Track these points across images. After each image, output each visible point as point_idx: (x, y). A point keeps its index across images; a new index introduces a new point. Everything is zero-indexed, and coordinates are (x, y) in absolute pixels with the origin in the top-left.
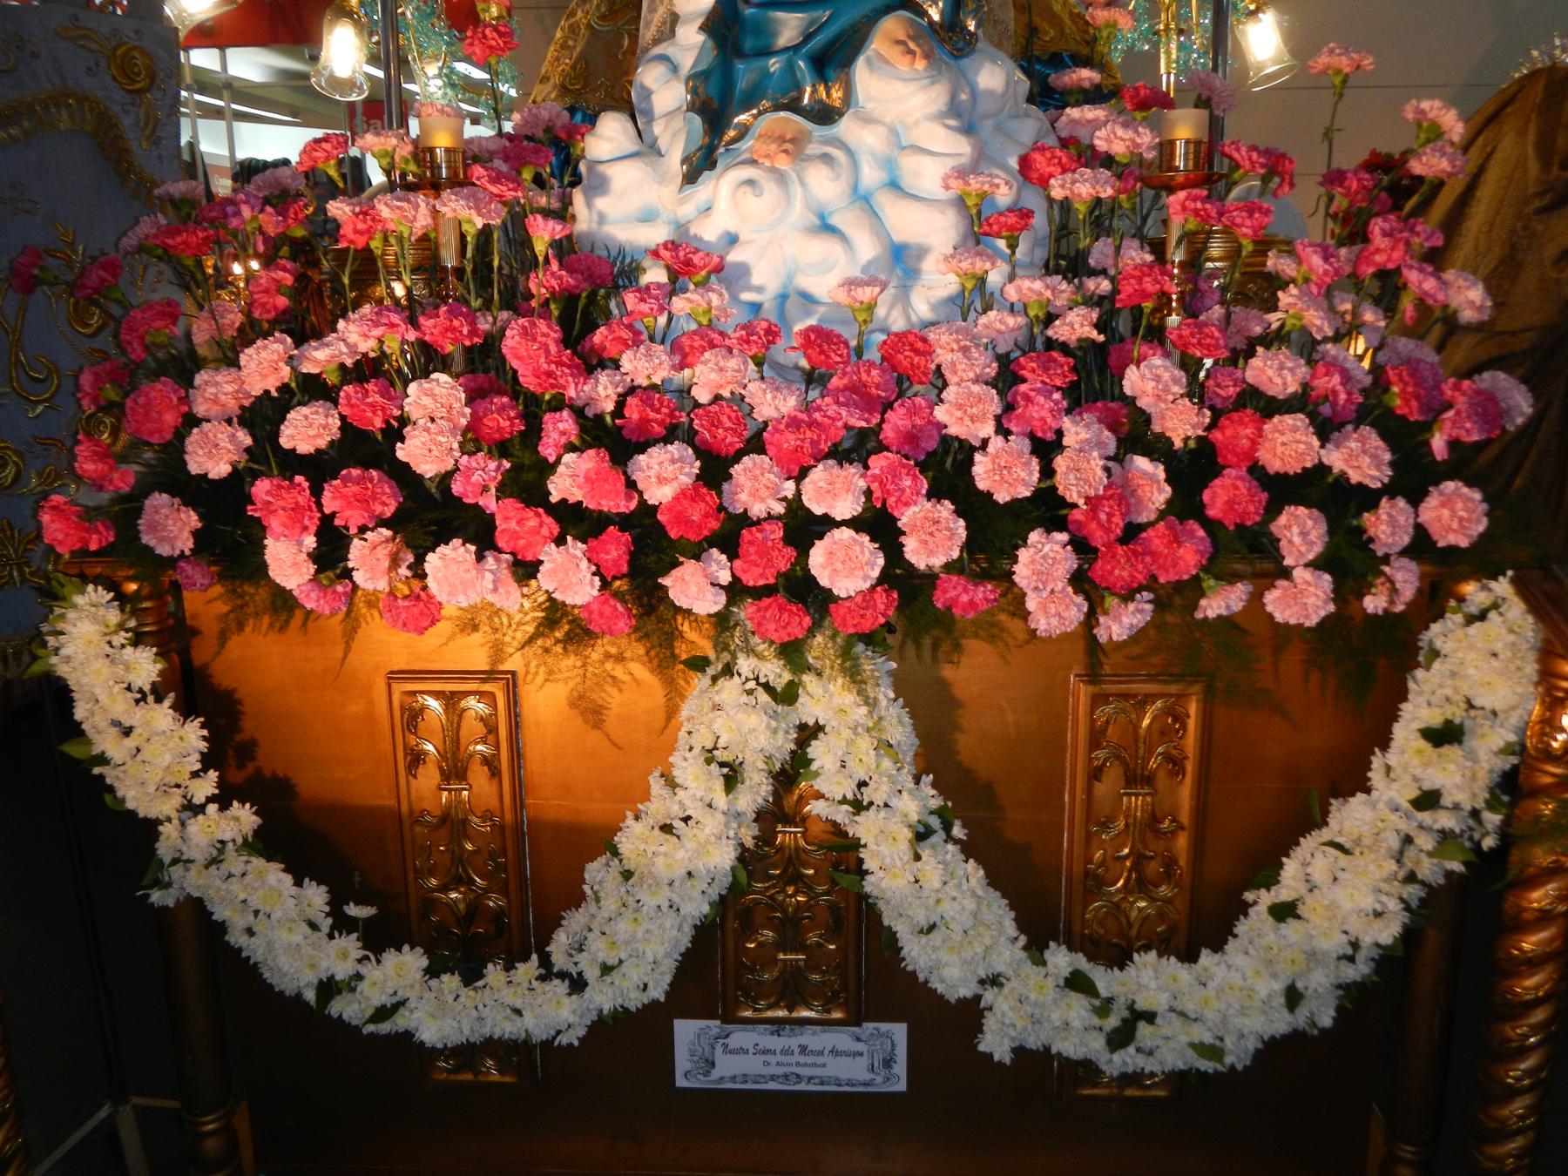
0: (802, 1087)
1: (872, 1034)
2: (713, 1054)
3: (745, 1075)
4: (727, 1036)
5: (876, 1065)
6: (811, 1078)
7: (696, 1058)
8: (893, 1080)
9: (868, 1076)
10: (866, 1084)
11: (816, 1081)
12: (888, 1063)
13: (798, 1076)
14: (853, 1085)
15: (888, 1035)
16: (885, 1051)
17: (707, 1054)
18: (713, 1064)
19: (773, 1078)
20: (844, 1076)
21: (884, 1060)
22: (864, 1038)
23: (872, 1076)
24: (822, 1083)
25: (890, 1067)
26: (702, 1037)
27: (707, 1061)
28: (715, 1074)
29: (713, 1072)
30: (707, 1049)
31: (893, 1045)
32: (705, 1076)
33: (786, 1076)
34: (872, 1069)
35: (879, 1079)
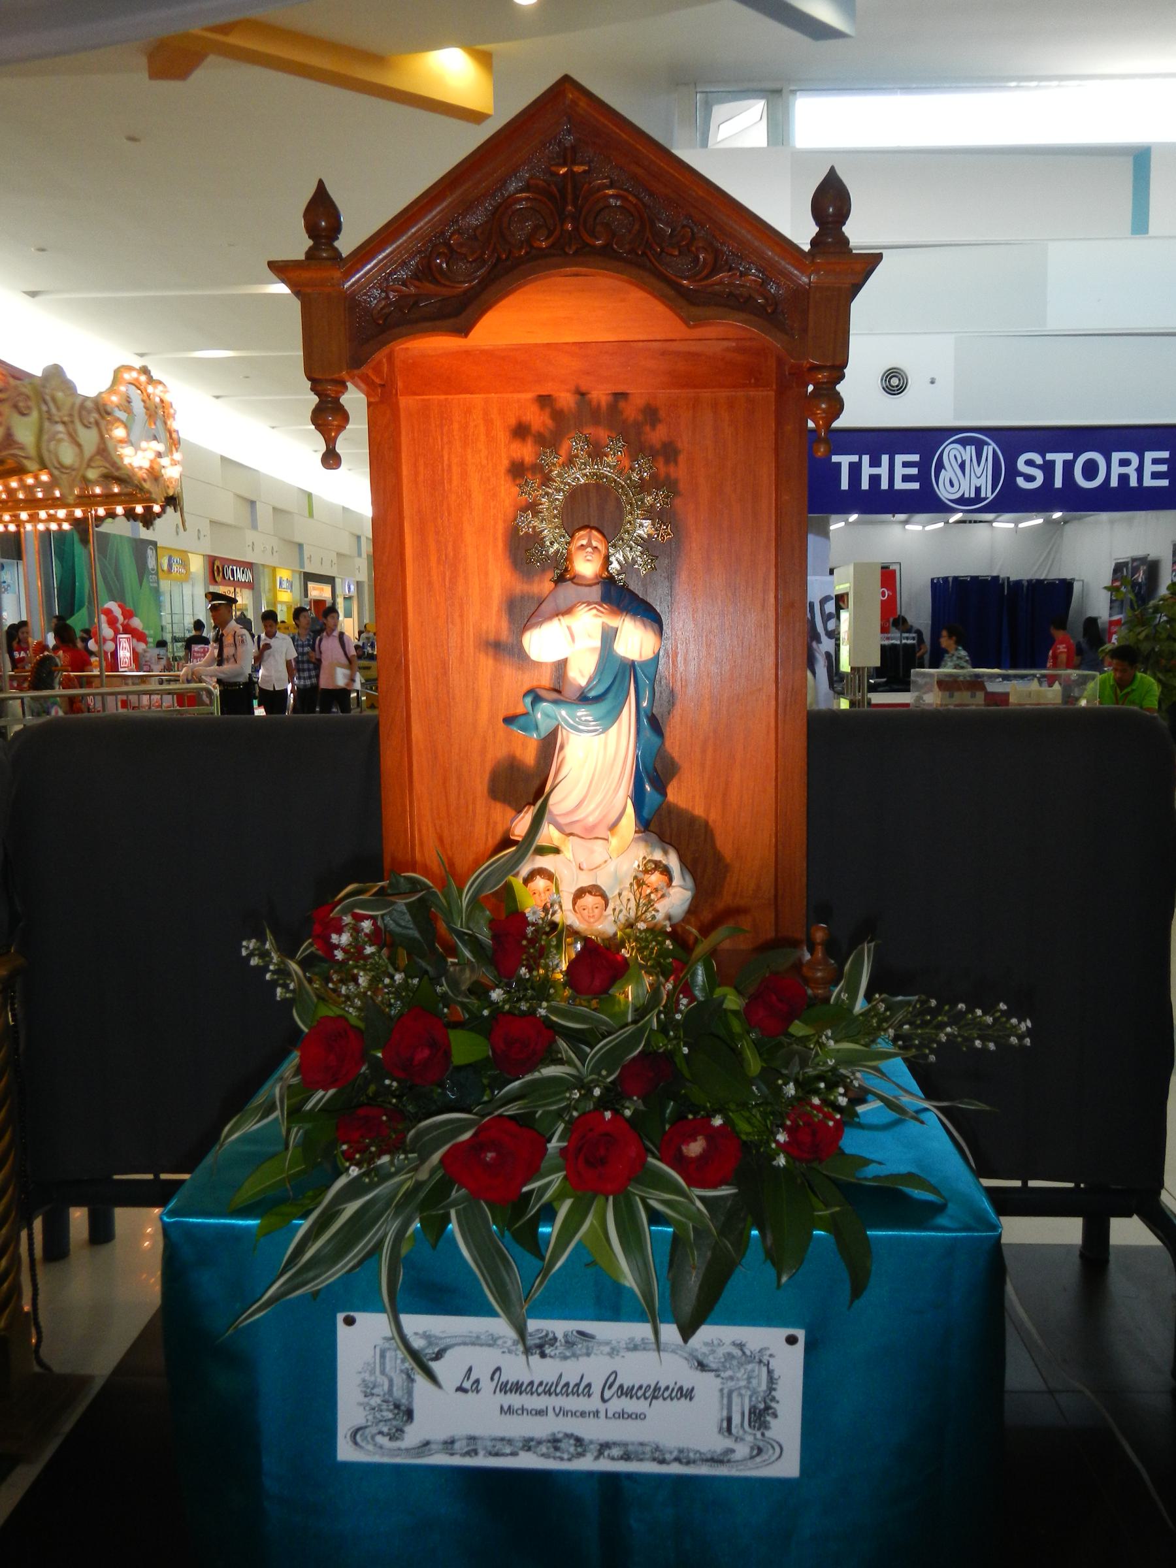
0: (586, 1464)
1: (730, 1356)
2: (410, 1393)
3: (472, 1439)
5: (736, 1420)
6: (604, 1447)
7: (375, 1401)
8: (770, 1454)
9: (718, 1443)
10: (714, 1460)
11: (616, 1452)
12: (760, 1416)
13: (579, 1441)
14: (688, 1463)
15: (761, 1359)
16: (754, 1392)
17: (398, 1393)
18: (409, 1414)
19: (528, 1444)
20: (670, 1441)
21: (753, 1410)
22: (714, 1366)
23: (728, 1443)
24: (626, 1457)
25: (764, 1426)
26: (388, 1354)
27: (397, 1406)
28: (413, 1435)
29: (408, 1429)
30: (399, 1380)
32: (392, 1438)
33: (555, 1442)
34: (727, 1427)
35: (742, 1451)
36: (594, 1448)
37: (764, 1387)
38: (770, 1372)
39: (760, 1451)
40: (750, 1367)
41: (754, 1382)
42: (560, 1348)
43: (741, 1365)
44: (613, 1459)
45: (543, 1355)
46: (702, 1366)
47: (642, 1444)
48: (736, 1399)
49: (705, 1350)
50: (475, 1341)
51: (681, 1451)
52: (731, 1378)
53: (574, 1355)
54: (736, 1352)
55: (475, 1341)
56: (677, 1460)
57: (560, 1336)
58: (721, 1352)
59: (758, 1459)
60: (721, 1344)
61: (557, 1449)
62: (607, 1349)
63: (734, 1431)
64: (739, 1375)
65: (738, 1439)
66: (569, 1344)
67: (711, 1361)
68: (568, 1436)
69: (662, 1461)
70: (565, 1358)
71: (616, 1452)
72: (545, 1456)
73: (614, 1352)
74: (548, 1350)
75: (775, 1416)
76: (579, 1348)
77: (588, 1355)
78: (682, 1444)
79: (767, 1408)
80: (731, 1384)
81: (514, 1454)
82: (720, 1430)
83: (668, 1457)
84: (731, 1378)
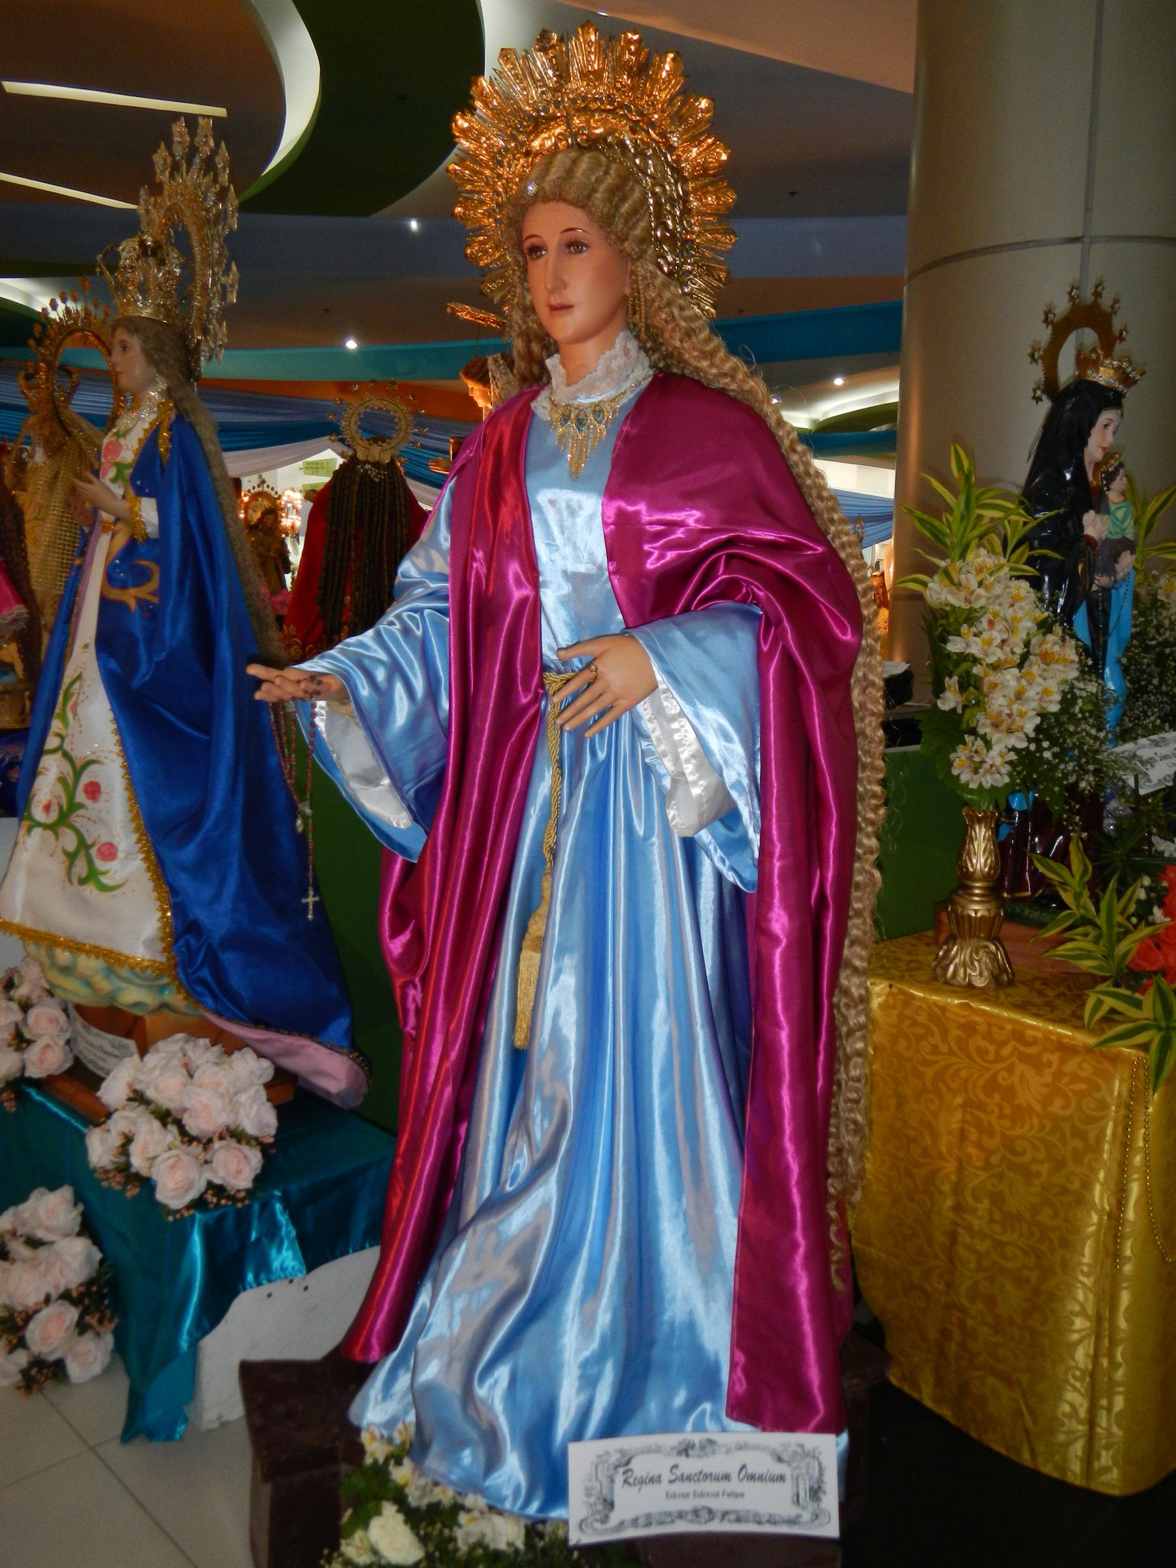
1: (795, 1453)
4: (628, 1462)
6: (725, 1514)
8: (824, 1519)
9: (791, 1511)
10: (792, 1522)
11: (732, 1517)
12: (816, 1493)
14: (775, 1523)
15: (813, 1455)
16: (811, 1478)
19: (681, 1515)
20: (765, 1509)
21: (811, 1489)
24: (739, 1520)
31: (821, 1469)
33: (696, 1512)
35: (806, 1516)
36: (719, 1515)
37: (816, 1473)
38: (820, 1464)
39: (817, 1517)
40: (808, 1460)
41: (811, 1470)
42: (697, 1451)
43: (802, 1458)
44: (730, 1521)
45: (687, 1455)
46: (780, 1460)
47: (748, 1511)
48: (801, 1482)
49: (781, 1449)
50: (648, 1451)
51: (770, 1516)
52: (797, 1467)
53: (706, 1455)
54: (799, 1450)
55: (648, 1451)
56: (770, 1522)
57: (697, 1442)
58: (790, 1450)
59: (816, 1522)
60: (790, 1445)
61: (697, 1516)
62: (724, 1450)
63: (801, 1501)
64: (803, 1465)
65: (803, 1508)
66: (703, 1448)
67: (785, 1456)
68: (704, 1508)
69: (759, 1523)
70: (699, 1457)
71: (732, 1517)
72: (691, 1521)
73: (728, 1451)
74: (690, 1452)
75: (825, 1493)
76: (708, 1450)
77: (714, 1453)
78: (772, 1511)
79: (820, 1488)
80: (797, 1472)
81: (673, 1522)
82: (793, 1502)
83: (764, 1519)
84: (797, 1467)
